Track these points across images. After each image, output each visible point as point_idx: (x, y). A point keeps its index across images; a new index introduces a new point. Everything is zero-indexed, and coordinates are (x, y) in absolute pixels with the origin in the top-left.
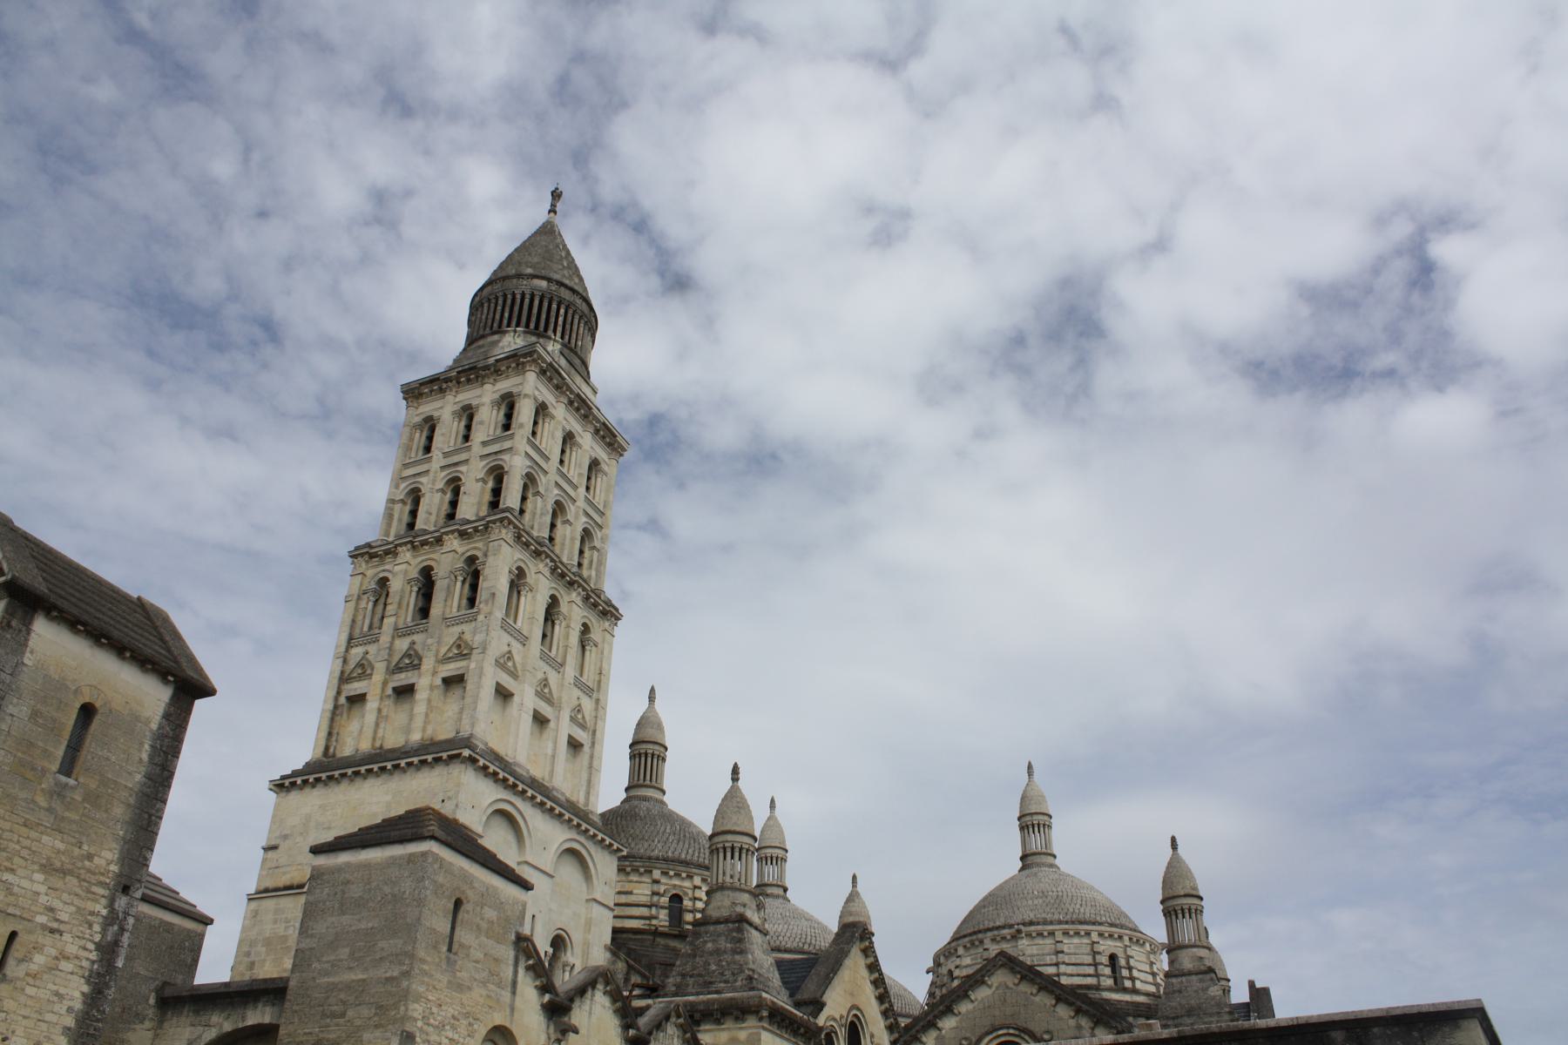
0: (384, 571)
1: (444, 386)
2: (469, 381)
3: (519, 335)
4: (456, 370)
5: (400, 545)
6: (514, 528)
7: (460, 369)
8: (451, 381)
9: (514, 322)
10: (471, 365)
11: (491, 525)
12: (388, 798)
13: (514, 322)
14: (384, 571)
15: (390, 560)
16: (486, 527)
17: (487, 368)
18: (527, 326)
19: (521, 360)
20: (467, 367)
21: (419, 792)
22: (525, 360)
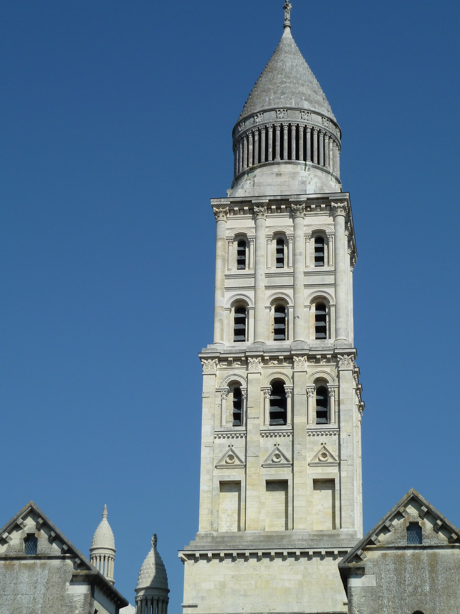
0: (234, 375)
1: (256, 209)
2: (279, 208)
3: (309, 168)
4: (269, 198)
5: (252, 357)
6: (348, 355)
7: (272, 198)
8: (262, 207)
9: (301, 156)
10: (283, 198)
11: (339, 356)
12: (299, 577)
13: (301, 156)
14: (234, 375)
15: (237, 366)
16: (335, 356)
17: (298, 203)
18: (312, 160)
19: (333, 204)
20: (279, 198)
21: (327, 576)
22: (336, 205)
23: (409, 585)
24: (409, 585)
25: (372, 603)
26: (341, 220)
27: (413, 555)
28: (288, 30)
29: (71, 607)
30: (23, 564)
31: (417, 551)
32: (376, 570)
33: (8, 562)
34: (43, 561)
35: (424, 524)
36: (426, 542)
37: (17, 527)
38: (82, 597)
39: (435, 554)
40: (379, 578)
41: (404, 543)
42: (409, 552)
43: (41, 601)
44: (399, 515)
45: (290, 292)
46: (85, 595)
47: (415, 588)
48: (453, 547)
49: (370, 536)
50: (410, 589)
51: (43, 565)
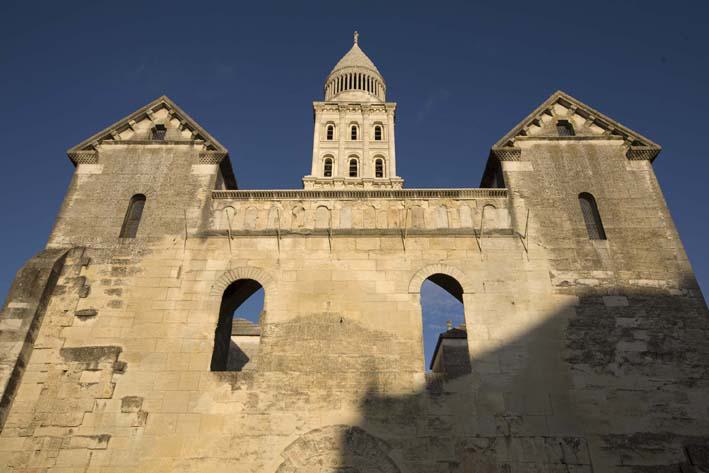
23: (570, 170)
24: (570, 170)
25: (531, 184)
26: (392, 117)
27: (568, 146)
28: (356, 45)
29: (195, 186)
30: (148, 149)
31: (572, 142)
32: (531, 157)
33: (131, 146)
34: (169, 146)
35: (574, 121)
36: (577, 135)
37: (147, 117)
38: (208, 178)
39: (592, 147)
40: (535, 163)
41: (557, 135)
42: (563, 143)
43: (162, 180)
44: (548, 112)
45: (360, 152)
46: (212, 176)
47: (577, 173)
48: (609, 139)
49: (522, 126)
50: (571, 173)
51: (169, 151)
